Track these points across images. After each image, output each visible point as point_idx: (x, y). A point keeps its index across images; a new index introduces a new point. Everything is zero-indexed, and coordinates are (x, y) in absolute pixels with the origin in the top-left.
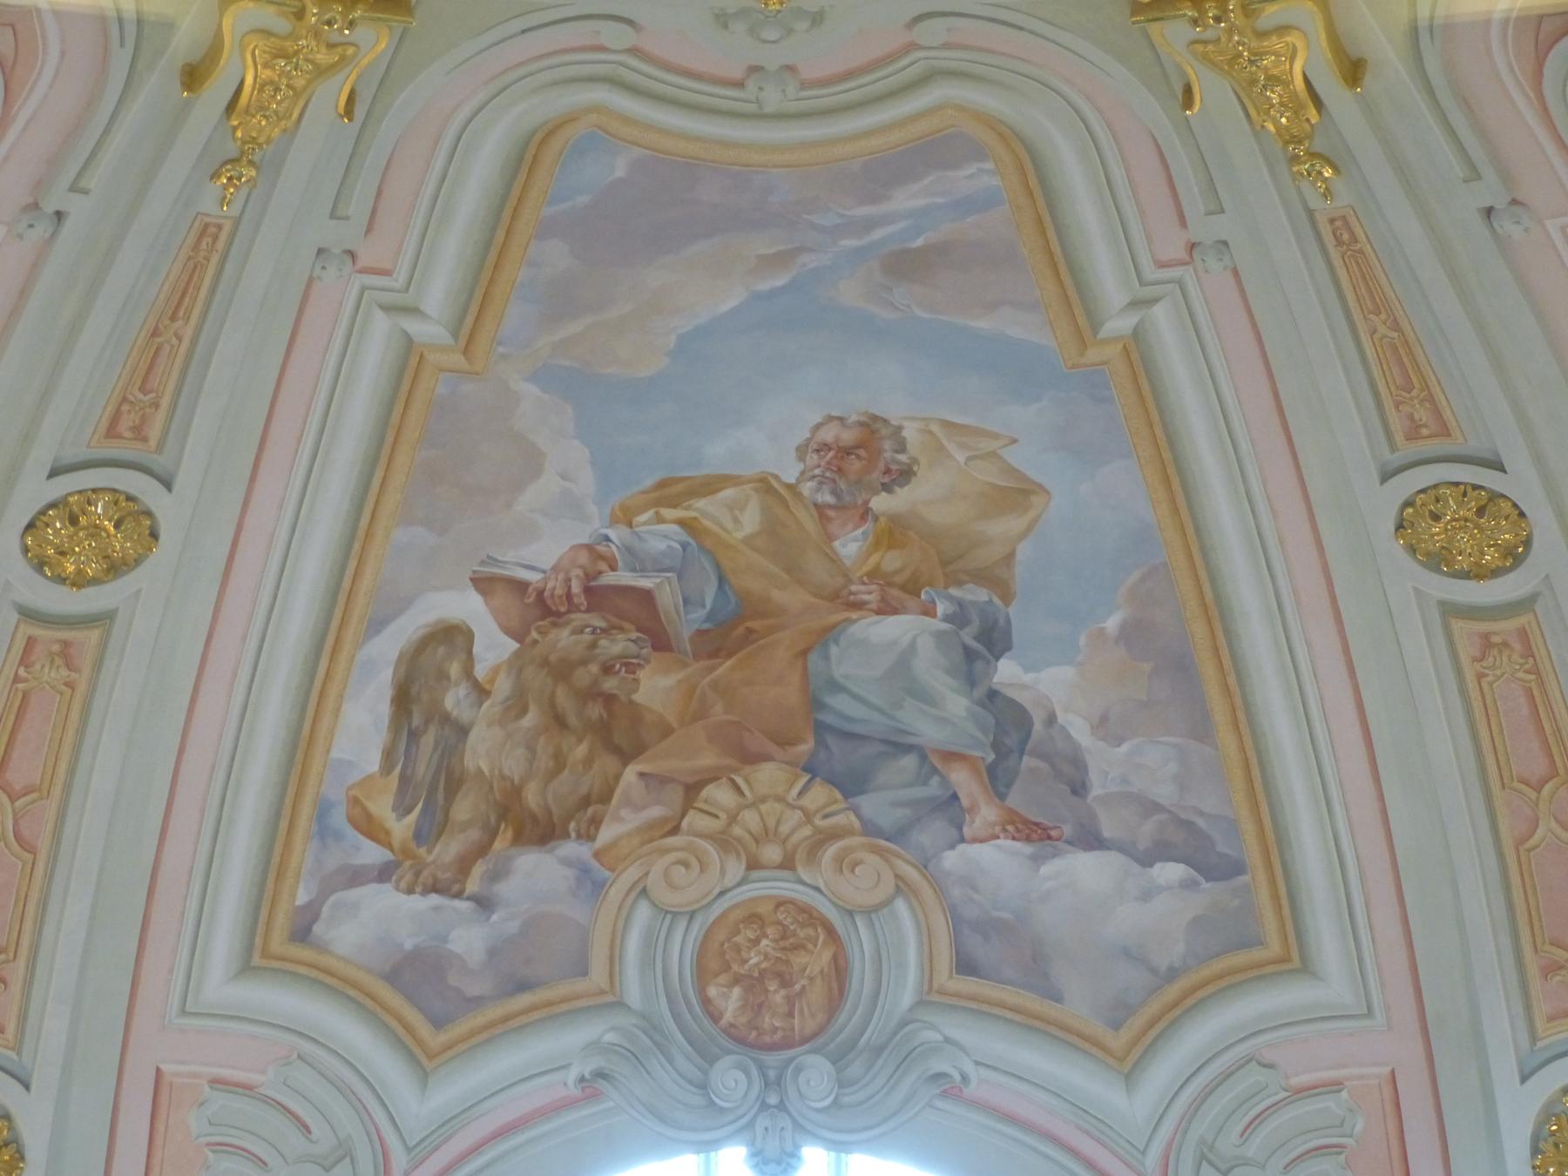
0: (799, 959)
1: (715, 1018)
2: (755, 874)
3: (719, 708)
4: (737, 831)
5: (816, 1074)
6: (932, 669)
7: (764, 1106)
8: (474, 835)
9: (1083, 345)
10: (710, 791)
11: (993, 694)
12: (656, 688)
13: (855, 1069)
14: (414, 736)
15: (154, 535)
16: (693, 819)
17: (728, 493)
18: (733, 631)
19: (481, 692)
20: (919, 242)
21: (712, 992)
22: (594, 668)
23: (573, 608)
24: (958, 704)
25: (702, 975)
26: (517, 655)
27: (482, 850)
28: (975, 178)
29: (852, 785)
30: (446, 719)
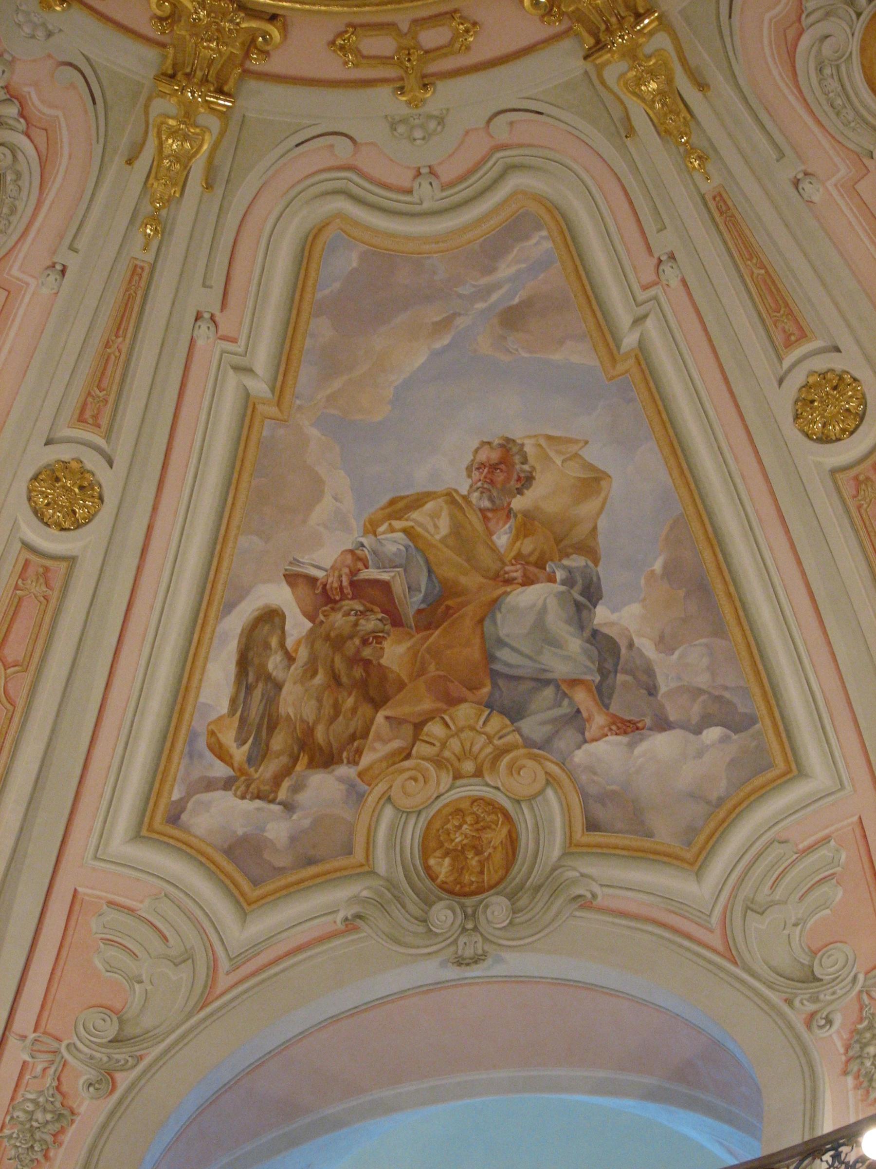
0: (487, 835)
1: (433, 879)
2: (459, 782)
3: (432, 667)
4: (447, 754)
5: (497, 908)
6: (558, 623)
7: (464, 930)
8: (284, 760)
9: (614, 361)
11: (595, 633)
12: (394, 654)
13: (521, 903)
14: (249, 689)
15: (101, 498)
16: (421, 748)
17: (430, 506)
19: (290, 659)
20: (516, 301)
21: (432, 862)
22: (357, 641)
23: (343, 597)
24: (575, 644)
25: (425, 853)
26: (311, 631)
27: (287, 771)
28: (540, 244)
29: (515, 713)
30: (269, 678)
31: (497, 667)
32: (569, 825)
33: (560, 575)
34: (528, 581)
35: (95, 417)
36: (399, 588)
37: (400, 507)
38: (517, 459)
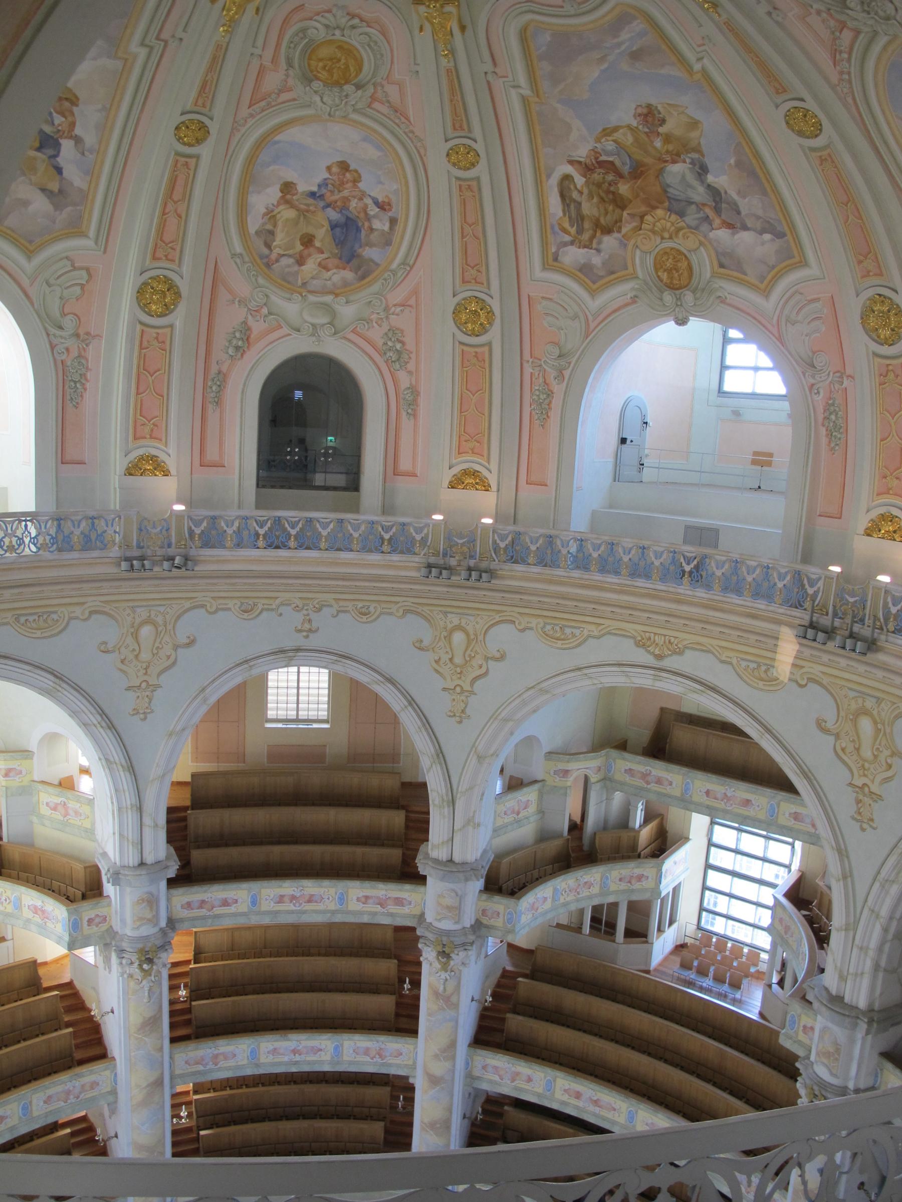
0: (679, 265)
1: (662, 281)
3: (641, 194)
5: (689, 297)
6: (691, 178)
7: (677, 305)
8: (591, 232)
10: (646, 217)
11: (709, 186)
12: (624, 189)
13: (698, 295)
14: (568, 206)
17: (621, 131)
18: (638, 172)
19: (581, 193)
20: (634, 48)
21: (659, 274)
22: (607, 184)
23: (595, 168)
24: (701, 189)
26: (586, 182)
27: (593, 236)
28: (638, 26)
29: (681, 214)
30: (575, 201)
31: (669, 195)
32: (712, 268)
33: (688, 160)
34: (674, 162)
35: (461, 127)
36: (618, 163)
37: (608, 132)
38: (656, 112)
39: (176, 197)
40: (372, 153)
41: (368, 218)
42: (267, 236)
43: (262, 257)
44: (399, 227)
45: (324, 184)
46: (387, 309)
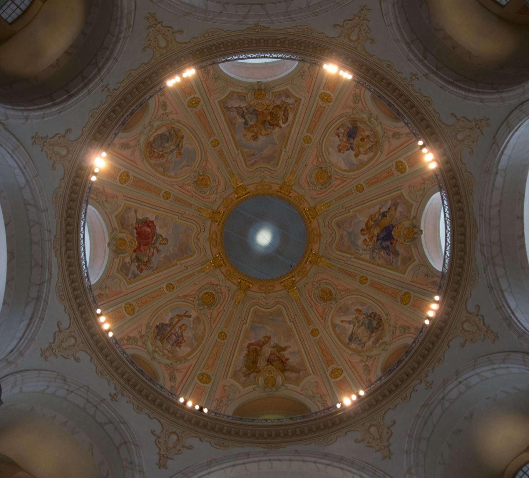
5: (256, 87)
6: (249, 120)
12: (269, 118)
24: (247, 117)
27: (283, 105)
29: (254, 110)
36: (268, 125)
37: (268, 134)
39: (377, 180)
40: (331, 150)
41: (344, 134)
42: (370, 149)
43: (376, 146)
44: (337, 126)
45: (348, 150)
46: (354, 109)
